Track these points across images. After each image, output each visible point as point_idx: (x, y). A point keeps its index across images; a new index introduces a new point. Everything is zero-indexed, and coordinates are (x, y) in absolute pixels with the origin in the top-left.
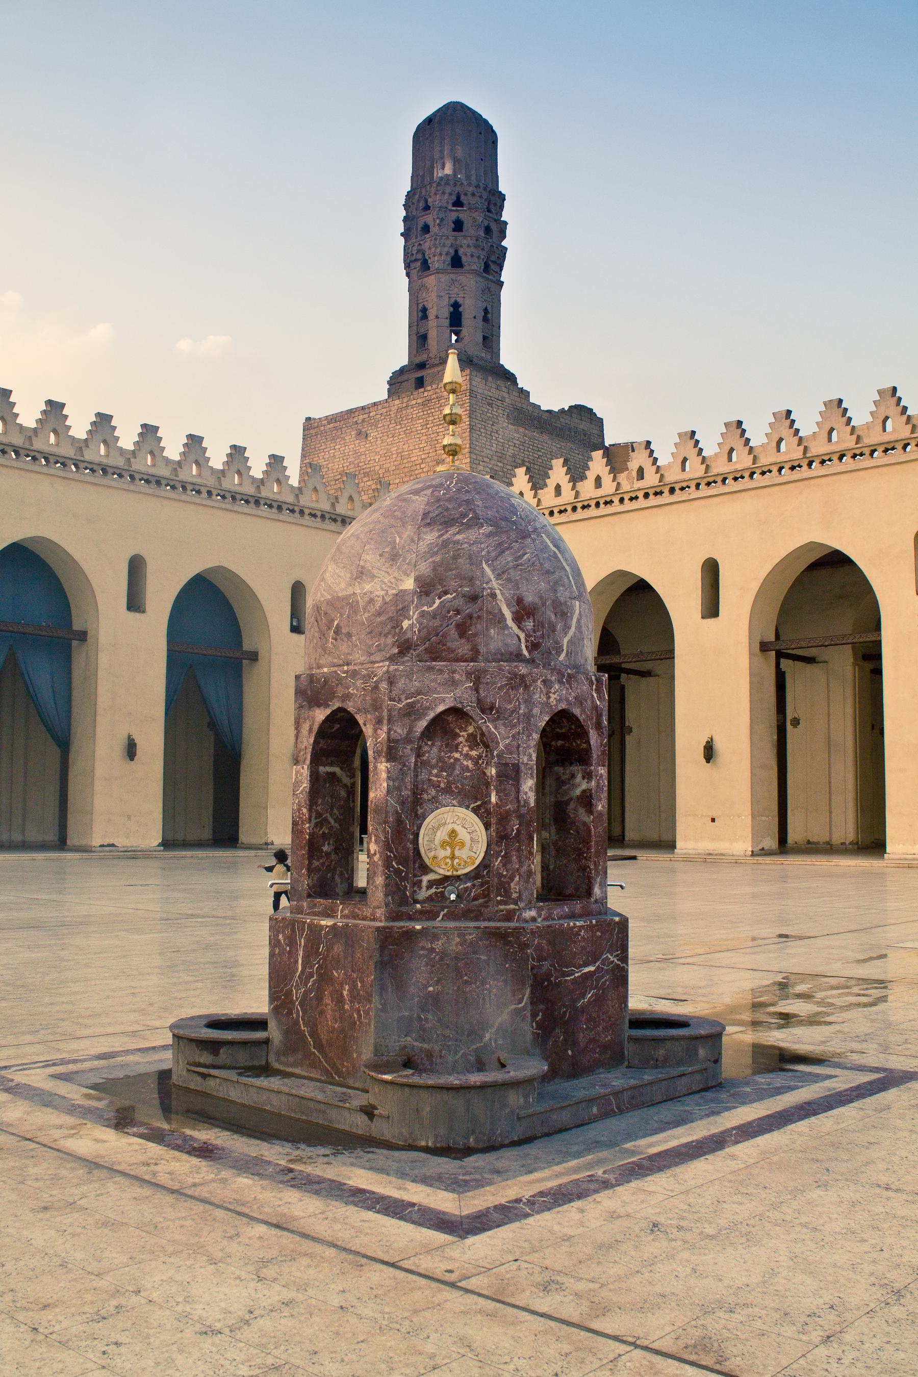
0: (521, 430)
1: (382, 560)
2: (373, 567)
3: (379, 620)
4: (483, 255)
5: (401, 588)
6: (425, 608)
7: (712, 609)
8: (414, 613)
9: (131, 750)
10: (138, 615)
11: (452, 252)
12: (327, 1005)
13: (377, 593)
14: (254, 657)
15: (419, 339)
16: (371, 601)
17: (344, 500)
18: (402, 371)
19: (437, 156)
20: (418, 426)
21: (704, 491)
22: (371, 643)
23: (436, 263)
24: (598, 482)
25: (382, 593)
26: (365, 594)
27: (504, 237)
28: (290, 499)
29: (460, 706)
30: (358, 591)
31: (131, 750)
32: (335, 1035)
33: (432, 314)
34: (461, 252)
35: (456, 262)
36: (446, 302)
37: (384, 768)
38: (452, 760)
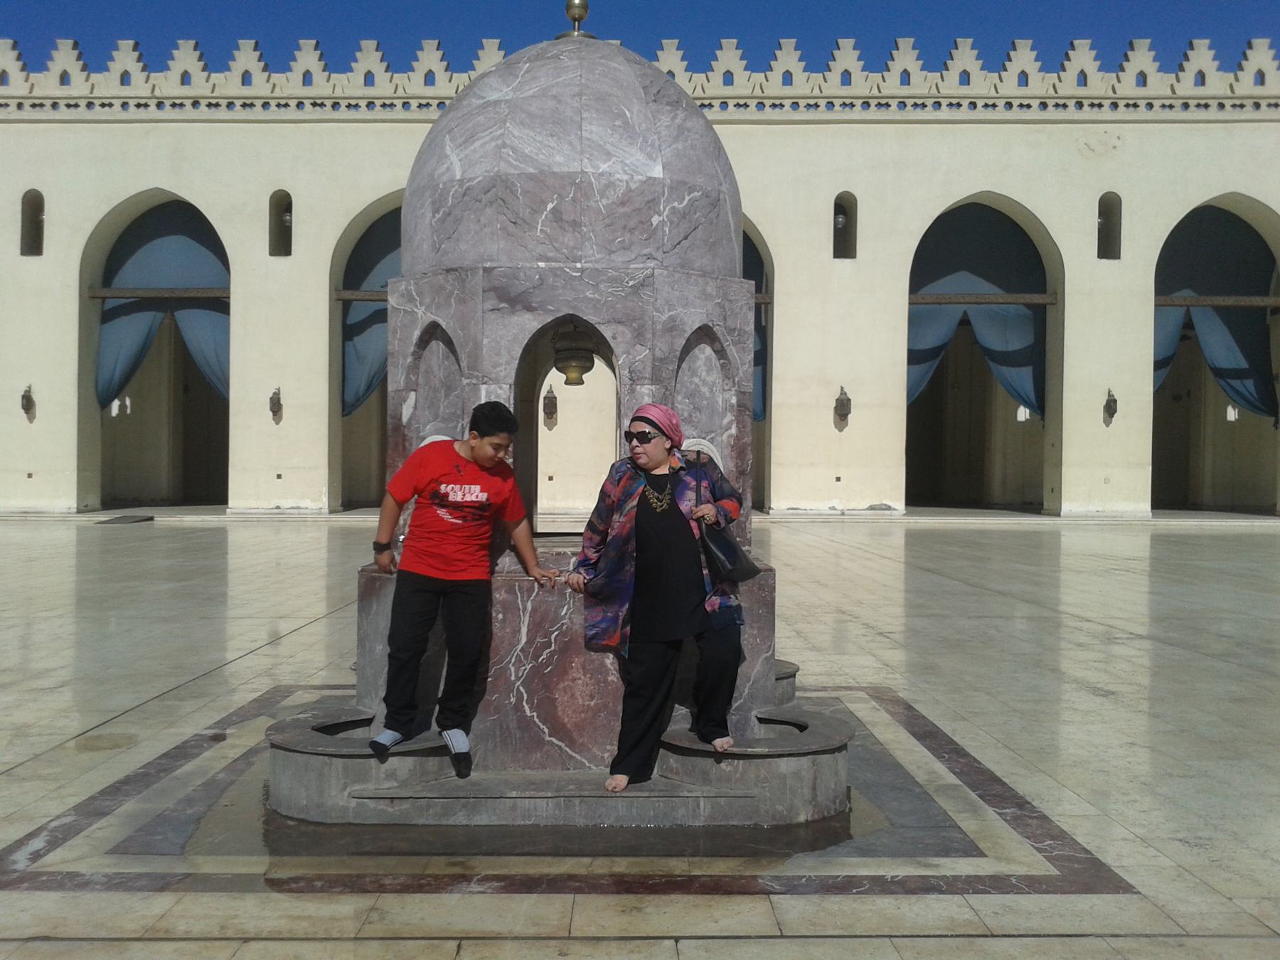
1: (617, 136)
2: (605, 142)
3: (621, 210)
5: (649, 175)
6: (676, 204)
8: (665, 208)
12: (574, 680)
13: (618, 176)
16: (611, 185)
22: (611, 238)
25: (626, 177)
26: (602, 175)
29: (710, 324)
30: (589, 170)
32: (590, 714)
37: (647, 392)
38: (693, 386)
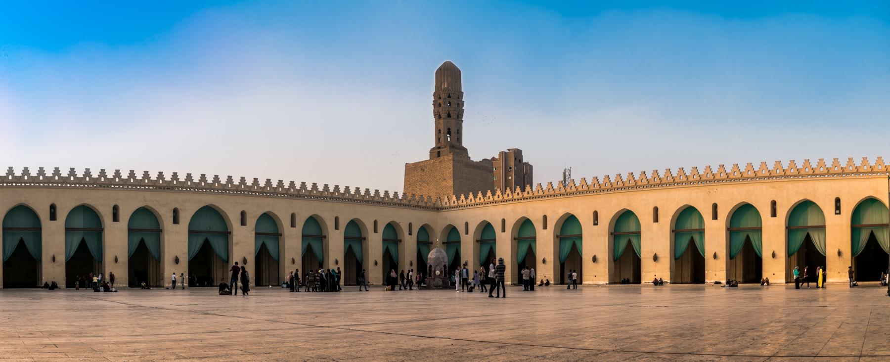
0: (468, 169)
4: (457, 113)
7: (504, 230)
9: (376, 263)
10: (376, 234)
11: (448, 113)
14: (400, 241)
15: (438, 140)
17: (420, 202)
18: (433, 149)
19: (443, 81)
20: (438, 168)
21: (503, 203)
23: (443, 116)
24: (480, 199)
27: (463, 106)
28: (408, 203)
31: (376, 263)
33: (442, 131)
34: (450, 112)
35: (449, 116)
36: (446, 128)
